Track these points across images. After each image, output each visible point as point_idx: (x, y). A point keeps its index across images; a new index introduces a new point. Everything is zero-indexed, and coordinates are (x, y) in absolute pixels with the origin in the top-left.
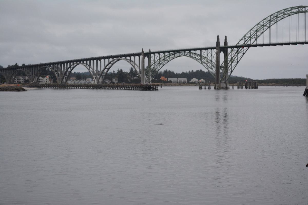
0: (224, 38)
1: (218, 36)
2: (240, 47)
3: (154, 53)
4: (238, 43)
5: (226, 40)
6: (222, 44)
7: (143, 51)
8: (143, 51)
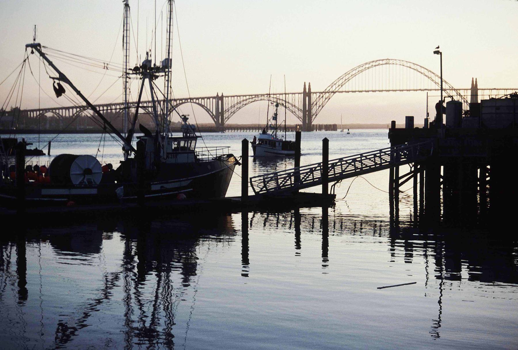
0: (304, 84)
1: (305, 83)
2: (326, 93)
3: (226, 97)
4: (326, 90)
5: (309, 86)
6: (307, 91)
7: (218, 95)
8: (218, 95)
